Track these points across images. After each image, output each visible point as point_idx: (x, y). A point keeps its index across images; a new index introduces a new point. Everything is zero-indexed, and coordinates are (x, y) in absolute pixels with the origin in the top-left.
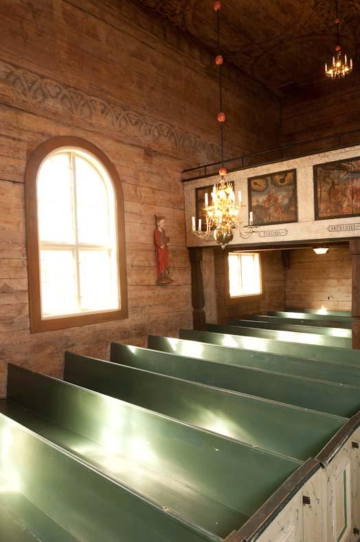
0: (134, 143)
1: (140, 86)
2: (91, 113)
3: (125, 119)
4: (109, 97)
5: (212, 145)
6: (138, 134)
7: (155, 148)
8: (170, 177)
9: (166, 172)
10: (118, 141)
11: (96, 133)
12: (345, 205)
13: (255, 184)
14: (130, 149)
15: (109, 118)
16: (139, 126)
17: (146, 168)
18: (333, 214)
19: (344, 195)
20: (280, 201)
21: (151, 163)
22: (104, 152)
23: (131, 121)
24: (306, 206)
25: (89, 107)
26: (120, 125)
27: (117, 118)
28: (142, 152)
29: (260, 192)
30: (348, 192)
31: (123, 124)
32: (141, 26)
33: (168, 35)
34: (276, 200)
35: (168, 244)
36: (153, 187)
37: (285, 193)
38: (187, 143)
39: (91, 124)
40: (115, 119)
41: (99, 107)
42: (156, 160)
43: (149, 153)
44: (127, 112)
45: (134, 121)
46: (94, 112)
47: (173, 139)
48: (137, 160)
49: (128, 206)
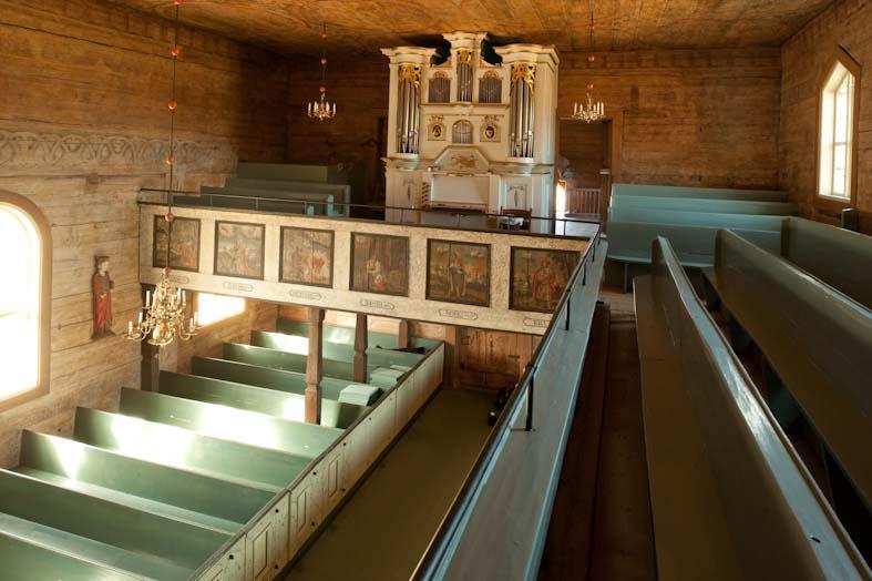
0: (72, 174)
1: (86, 98)
2: (14, 153)
3: (62, 147)
4: (42, 125)
5: (185, 145)
6: (79, 161)
7: (103, 171)
8: (121, 201)
9: (117, 197)
10: (49, 178)
11: (19, 176)
12: (306, 272)
13: (223, 228)
14: (66, 183)
15: (39, 152)
16: (80, 150)
17: (88, 199)
18: (295, 279)
19: (306, 262)
20: (247, 253)
21: (94, 192)
22: (30, 198)
23: (69, 147)
24: (271, 268)
25: (12, 146)
26: (54, 157)
27: (51, 150)
28: (84, 181)
29: (228, 240)
30: (310, 261)
31: (59, 154)
32: (93, 23)
33: (131, 23)
34: (244, 251)
35: (112, 291)
36: (95, 220)
37: (254, 248)
38: (148, 152)
39: (12, 168)
40: (47, 150)
41: (25, 144)
42: (101, 187)
43: (92, 181)
44: (64, 139)
45: (73, 147)
46: (17, 151)
47: (129, 153)
48: (77, 193)
49: (58, 254)
